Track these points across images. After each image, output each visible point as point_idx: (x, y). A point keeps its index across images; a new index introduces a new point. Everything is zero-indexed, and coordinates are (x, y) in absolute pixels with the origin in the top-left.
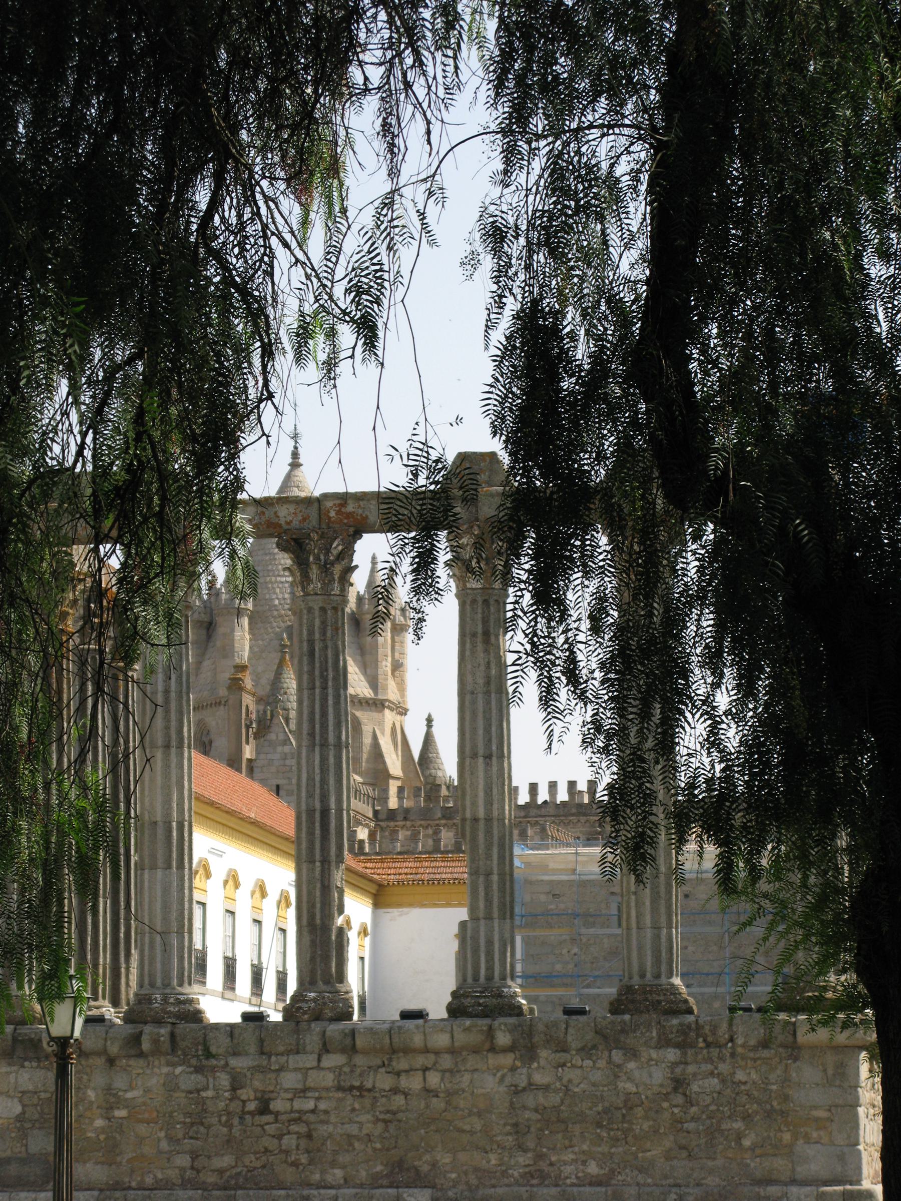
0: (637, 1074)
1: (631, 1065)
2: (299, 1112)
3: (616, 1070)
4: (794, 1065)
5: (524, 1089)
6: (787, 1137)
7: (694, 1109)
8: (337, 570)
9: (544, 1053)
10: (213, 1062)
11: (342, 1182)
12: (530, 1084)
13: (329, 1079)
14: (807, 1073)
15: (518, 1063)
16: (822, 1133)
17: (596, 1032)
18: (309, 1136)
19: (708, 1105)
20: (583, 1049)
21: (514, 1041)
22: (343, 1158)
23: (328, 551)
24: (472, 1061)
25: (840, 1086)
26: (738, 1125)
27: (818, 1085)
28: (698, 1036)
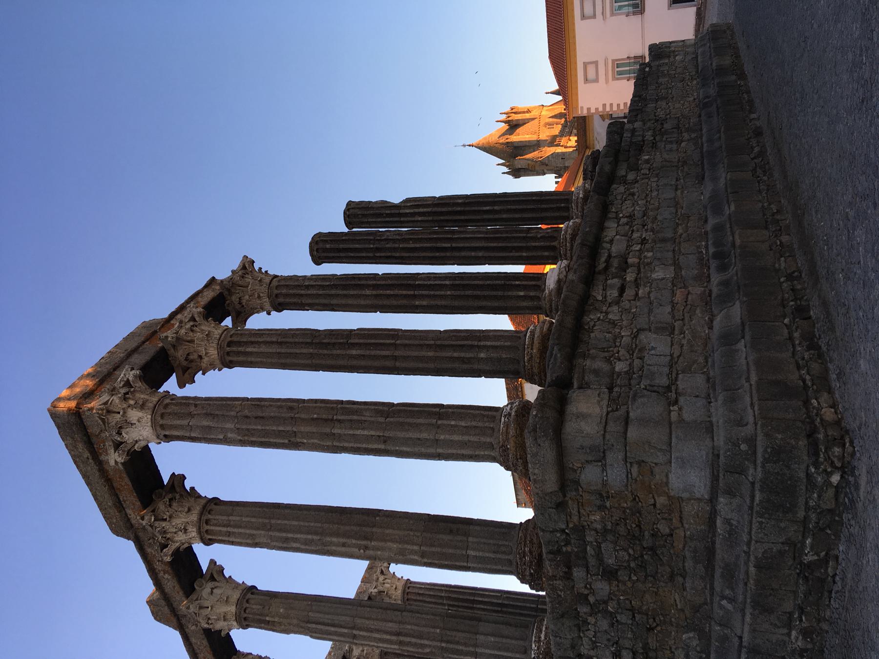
0: (598, 599)
1: (592, 599)
4: (584, 487)
7: (632, 565)
9: (586, 652)
14: (590, 475)
17: (562, 616)
19: (629, 555)
25: (604, 452)
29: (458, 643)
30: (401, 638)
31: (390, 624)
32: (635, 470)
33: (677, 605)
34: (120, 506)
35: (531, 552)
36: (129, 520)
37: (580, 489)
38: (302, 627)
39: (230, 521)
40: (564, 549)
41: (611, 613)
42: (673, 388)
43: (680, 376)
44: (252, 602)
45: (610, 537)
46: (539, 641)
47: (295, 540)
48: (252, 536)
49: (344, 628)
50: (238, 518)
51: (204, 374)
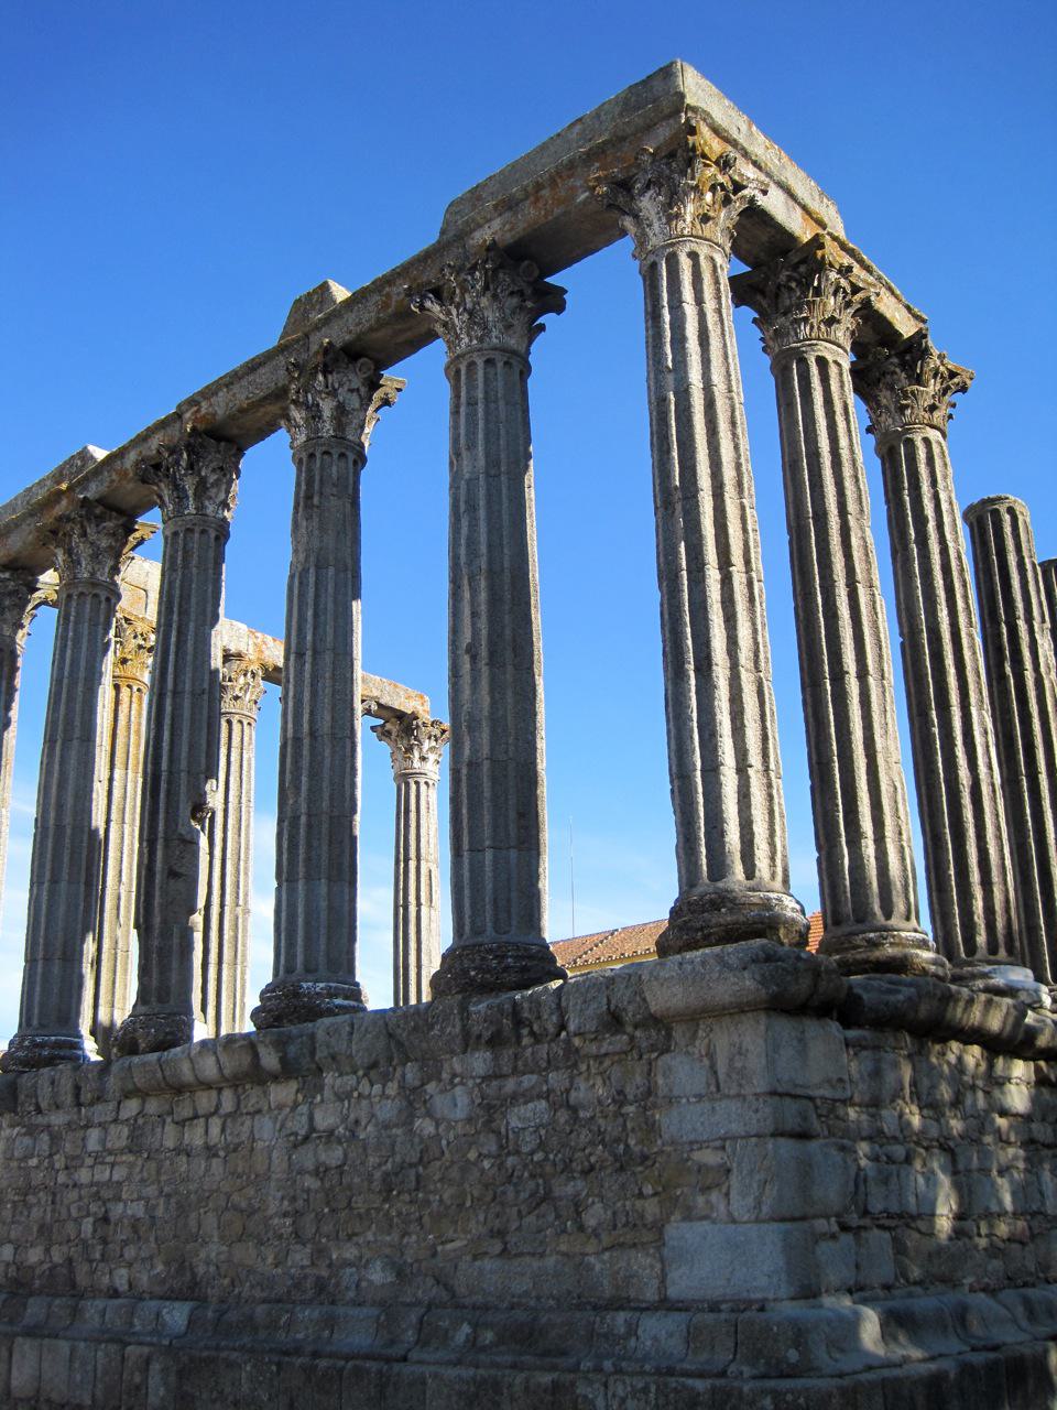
1: (431, 1087)
2: (97, 1184)
3: (413, 1100)
5: (306, 1138)
6: (651, 1208)
7: (511, 1161)
8: (189, 485)
9: (329, 1078)
10: (40, 1120)
11: (126, 1287)
12: (312, 1129)
13: (119, 1136)
15: (300, 1097)
16: (714, 1196)
17: (390, 1036)
18: (106, 1219)
19: (532, 1153)
20: (374, 1065)
21: (283, 1061)
22: (130, 1252)
23: (177, 462)
24: (253, 1097)
26: (576, 1187)
27: (700, 1097)
28: (518, 1022)
29: (309, 846)
30: (306, 741)
31: (328, 717)
32: (709, 1157)
33: (443, 1243)
34: (508, 205)
35: (507, 969)
36: (480, 226)
37: (655, 1055)
38: (307, 557)
39: (496, 401)
40: (525, 1031)
41: (412, 1123)
42: (867, 1222)
43: (887, 1235)
44: (342, 464)
45: (563, 1116)
46: (332, 994)
47: (473, 526)
48: (471, 446)
49: (314, 634)
50: (503, 416)
51: (755, 321)
